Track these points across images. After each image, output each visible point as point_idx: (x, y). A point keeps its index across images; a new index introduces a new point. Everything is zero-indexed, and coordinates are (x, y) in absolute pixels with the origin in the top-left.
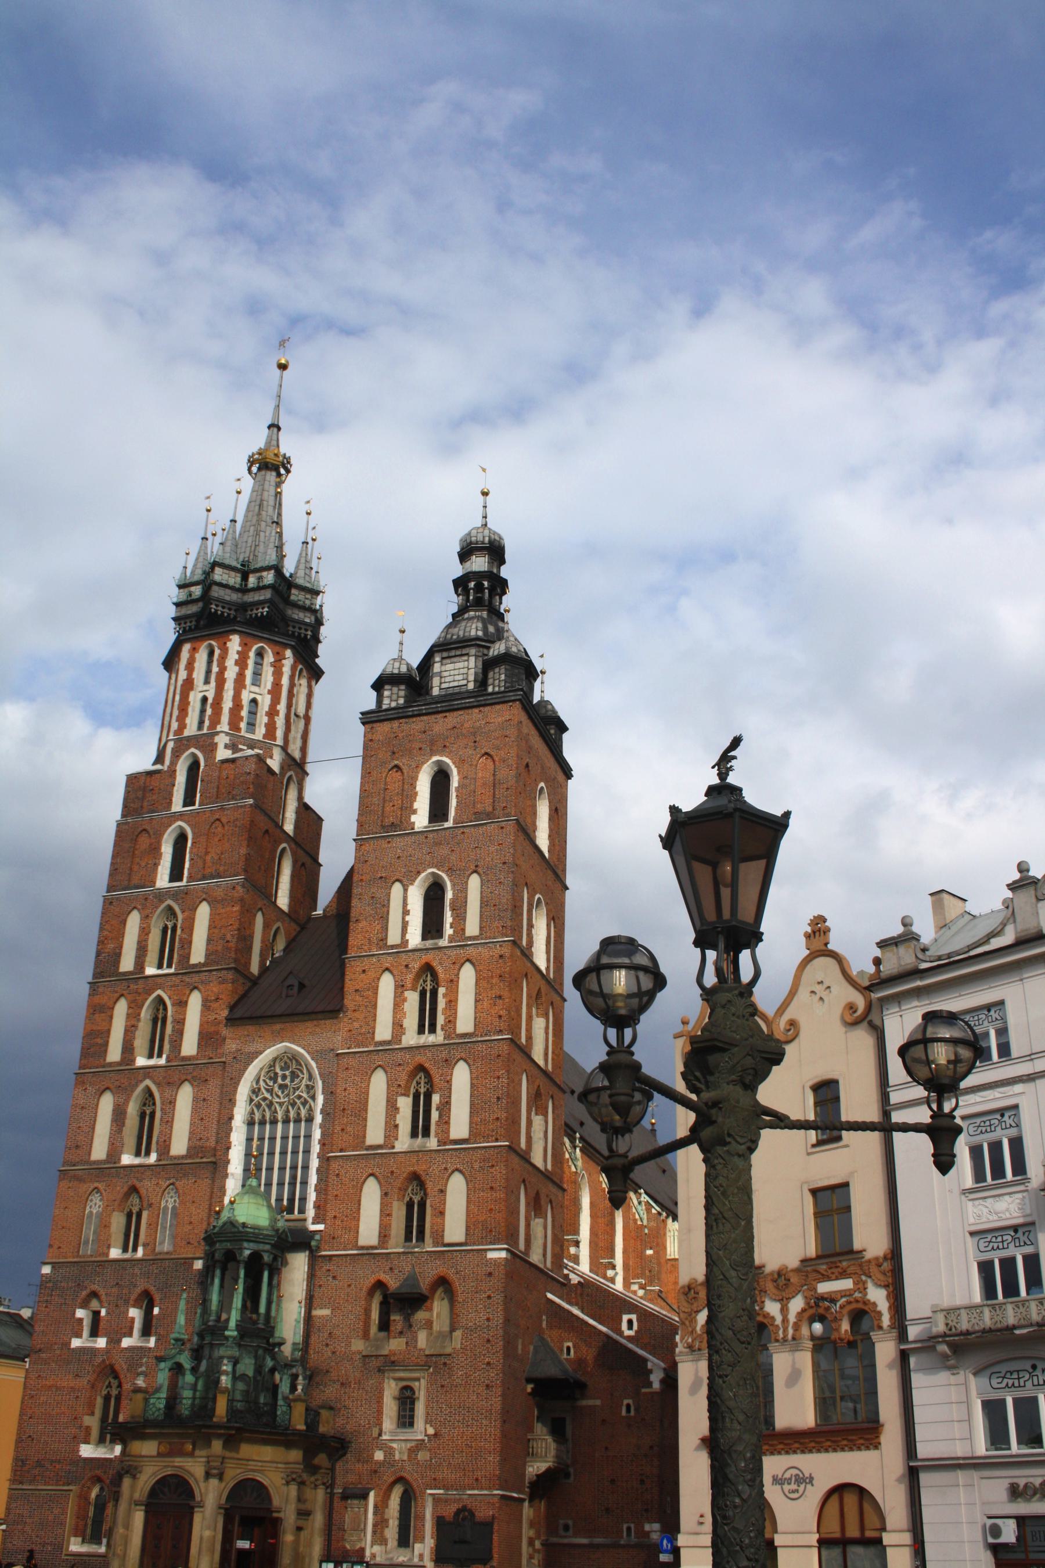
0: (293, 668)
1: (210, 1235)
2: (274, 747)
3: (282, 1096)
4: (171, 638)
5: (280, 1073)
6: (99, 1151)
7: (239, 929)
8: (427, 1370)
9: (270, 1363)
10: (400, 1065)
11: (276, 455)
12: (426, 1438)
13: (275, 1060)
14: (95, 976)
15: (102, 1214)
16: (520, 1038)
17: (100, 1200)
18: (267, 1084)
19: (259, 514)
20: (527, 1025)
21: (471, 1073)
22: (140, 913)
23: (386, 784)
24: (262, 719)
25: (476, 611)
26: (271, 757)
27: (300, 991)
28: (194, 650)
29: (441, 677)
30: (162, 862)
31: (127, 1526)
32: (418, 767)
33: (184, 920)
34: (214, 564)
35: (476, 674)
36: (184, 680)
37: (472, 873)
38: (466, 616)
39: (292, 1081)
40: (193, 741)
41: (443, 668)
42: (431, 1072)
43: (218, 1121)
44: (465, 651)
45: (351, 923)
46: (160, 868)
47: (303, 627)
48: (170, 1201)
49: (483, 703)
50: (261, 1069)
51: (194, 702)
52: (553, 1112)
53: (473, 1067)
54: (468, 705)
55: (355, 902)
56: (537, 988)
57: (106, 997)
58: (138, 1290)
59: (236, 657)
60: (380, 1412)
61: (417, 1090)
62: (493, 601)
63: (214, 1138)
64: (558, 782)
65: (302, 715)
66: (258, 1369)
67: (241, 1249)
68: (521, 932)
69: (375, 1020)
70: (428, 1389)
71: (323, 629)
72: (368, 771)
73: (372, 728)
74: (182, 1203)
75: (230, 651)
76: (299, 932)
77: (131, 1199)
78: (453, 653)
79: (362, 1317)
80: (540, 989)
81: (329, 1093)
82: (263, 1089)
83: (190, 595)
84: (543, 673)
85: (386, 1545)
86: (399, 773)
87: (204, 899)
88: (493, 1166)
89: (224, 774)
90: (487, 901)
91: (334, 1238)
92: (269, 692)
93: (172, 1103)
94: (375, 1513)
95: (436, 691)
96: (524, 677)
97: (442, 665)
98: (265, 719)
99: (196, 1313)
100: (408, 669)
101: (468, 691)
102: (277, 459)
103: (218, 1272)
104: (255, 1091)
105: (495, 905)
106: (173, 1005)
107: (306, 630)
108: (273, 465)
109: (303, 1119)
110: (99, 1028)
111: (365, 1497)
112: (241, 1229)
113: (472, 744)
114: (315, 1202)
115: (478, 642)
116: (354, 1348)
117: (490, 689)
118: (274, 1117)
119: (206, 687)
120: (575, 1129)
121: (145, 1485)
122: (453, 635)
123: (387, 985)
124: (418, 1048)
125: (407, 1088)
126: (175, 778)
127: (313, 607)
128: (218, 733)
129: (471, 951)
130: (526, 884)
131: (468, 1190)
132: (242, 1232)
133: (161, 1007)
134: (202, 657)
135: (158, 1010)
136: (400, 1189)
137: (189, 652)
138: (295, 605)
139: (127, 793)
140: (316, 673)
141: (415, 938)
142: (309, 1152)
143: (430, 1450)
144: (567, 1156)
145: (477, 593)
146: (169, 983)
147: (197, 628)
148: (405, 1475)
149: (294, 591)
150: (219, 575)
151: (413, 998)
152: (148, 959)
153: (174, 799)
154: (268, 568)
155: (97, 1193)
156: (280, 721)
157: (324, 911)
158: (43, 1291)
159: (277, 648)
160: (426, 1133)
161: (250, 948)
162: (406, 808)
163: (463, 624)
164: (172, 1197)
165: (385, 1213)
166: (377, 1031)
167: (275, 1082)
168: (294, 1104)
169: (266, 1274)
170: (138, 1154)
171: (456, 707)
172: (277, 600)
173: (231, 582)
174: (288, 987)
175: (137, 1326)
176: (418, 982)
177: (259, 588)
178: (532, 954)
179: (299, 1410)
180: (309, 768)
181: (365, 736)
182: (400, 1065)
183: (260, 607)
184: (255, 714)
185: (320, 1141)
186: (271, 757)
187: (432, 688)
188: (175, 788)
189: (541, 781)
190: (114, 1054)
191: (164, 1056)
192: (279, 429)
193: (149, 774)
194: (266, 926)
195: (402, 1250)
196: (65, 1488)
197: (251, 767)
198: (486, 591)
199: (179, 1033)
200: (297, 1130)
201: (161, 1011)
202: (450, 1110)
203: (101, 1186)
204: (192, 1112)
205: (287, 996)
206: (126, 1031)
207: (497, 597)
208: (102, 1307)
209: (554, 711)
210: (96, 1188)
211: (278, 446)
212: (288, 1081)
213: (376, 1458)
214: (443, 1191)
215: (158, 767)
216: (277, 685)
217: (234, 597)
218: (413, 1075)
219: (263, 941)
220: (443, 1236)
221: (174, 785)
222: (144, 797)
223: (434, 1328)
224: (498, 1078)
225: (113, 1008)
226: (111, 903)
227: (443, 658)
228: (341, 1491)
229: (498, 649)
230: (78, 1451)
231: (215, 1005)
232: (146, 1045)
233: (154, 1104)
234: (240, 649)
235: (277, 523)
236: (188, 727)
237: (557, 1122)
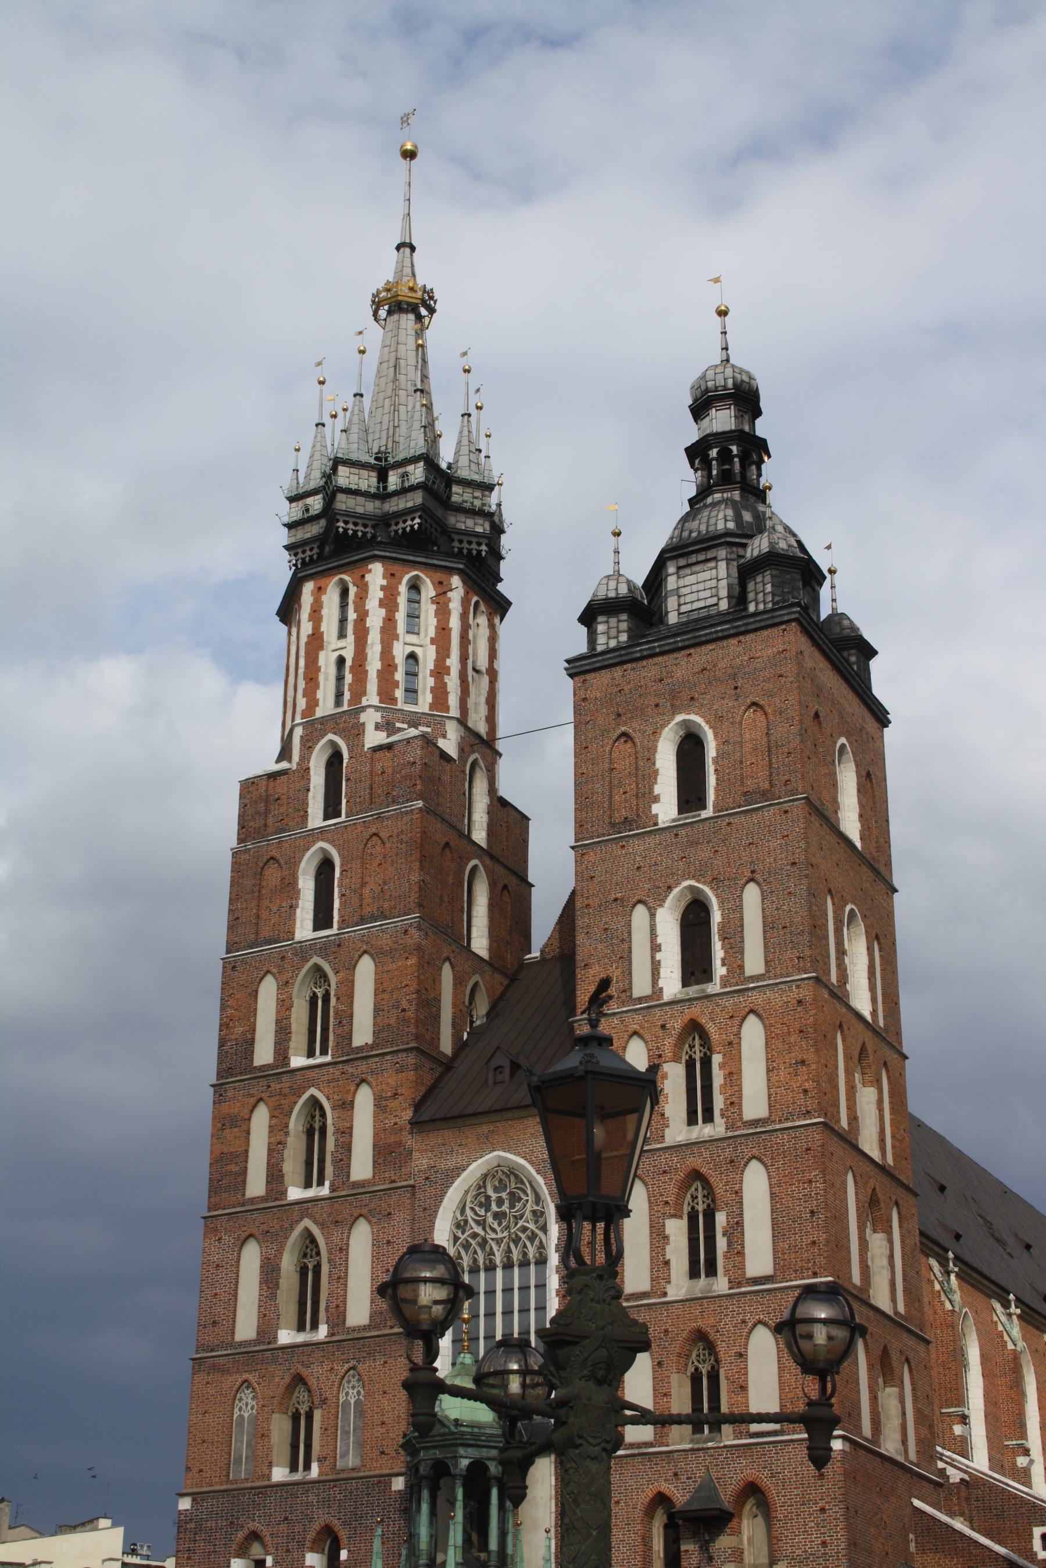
0: (465, 602)
1: (409, 1441)
2: (447, 721)
3: (498, 1229)
4: (285, 575)
5: (494, 1196)
6: (246, 1328)
7: (418, 992)
10: (665, 1172)
11: (411, 289)
13: (485, 1177)
14: (220, 1074)
15: (257, 1418)
16: (839, 1121)
17: (253, 1398)
18: (476, 1214)
19: (395, 380)
20: (847, 1100)
21: (770, 1178)
22: (276, 979)
23: (611, 762)
24: (426, 682)
25: (723, 491)
26: (444, 737)
27: (513, 1073)
28: (320, 590)
29: (679, 597)
30: (300, 902)
32: (656, 733)
33: (339, 984)
34: (337, 462)
35: (730, 587)
36: (309, 636)
37: (748, 882)
38: (709, 500)
39: (512, 1206)
41: (681, 583)
42: (712, 1180)
44: (710, 554)
45: (578, 970)
46: (298, 911)
47: (474, 540)
48: (351, 1394)
49: (743, 629)
50: (467, 1192)
51: (326, 666)
52: (900, 1227)
53: (772, 1169)
54: (720, 634)
55: (581, 939)
56: (860, 1044)
57: (238, 1105)
58: (317, 1526)
59: (381, 594)
61: (693, 1208)
62: (748, 474)
64: (867, 733)
65: (483, 669)
67: (456, 1458)
68: (827, 964)
71: (505, 540)
72: (584, 745)
73: (585, 680)
74: (368, 1395)
75: (371, 588)
76: (508, 987)
77: (296, 1394)
78: (693, 559)
79: (640, 1549)
80: (864, 1043)
82: (470, 1220)
83: (307, 510)
84: (832, 572)
86: (629, 744)
87: (365, 952)
89: (378, 767)
90: (773, 923)
92: (433, 641)
95: (673, 618)
96: (800, 584)
97: (679, 578)
98: (431, 682)
99: (400, 1555)
100: (629, 590)
101: (720, 614)
102: (414, 295)
103: (425, 1494)
105: (784, 927)
106: (333, 1108)
107: (479, 544)
108: (408, 303)
109: (532, 1260)
110: (232, 1150)
112: (453, 1429)
113: (733, 692)
117: (752, 608)
118: (491, 1260)
119: (341, 643)
120: (947, 1245)
122: (691, 532)
124: (688, 1145)
125: (679, 1205)
126: (309, 779)
127: (486, 508)
128: (363, 709)
129: (755, 998)
130: (830, 891)
132: (454, 1433)
133: (317, 1113)
135: (313, 1117)
136: (679, 1355)
137: (312, 594)
138: (460, 509)
139: (243, 806)
140: (500, 606)
141: (671, 984)
142: (545, 1308)
144: (937, 1287)
145: (723, 464)
146: (326, 1078)
147: (321, 557)
150: (345, 477)
152: (292, 1044)
153: (310, 810)
154: (414, 460)
155: (247, 1388)
156: (452, 682)
157: (542, 951)
158: (182, 1535)
159: (439, 576)
160: (711, 1270)
161: (436, 1018)
162: (644, 795)
163: (706, 513)
164: (353, 1387)
167: (487, 1210)
168: (516, 1240)
169: (494, 1493)
170: (301, 1328)
171: (703, 639)
172: (432, 505)
173: (364, 486)
174: (496, 1069)
176: (682, 1049)
177: (403, 491)
178: (847, 994)
180: (500, 746)
181: (575, 695)
182: (665, 1172)
183: (409, 518)
186: (444, 737)
187: (667, 613)
188: (311, 794)
189: (841, 735)
190: (256, 1185)
191: (327, 1183)
192: (413, 249)
193: (273, 776)
194: (458, 982)
195: (690, 1446)
197: (416, 753)
198: (736, 460)
200: (524, 1277)
201: (317, 1118)
203: (252, 1378)
204: (373, 1262)
205: (495, 1083)
206: (270, 1152)
207: (754, 467)
208: (267, 1553)
209: (853, 628)
210: (246, 1381)
211: (414, 275)
212: (505, 1208)
214: (742, 1355)
215: (284, 765)
216: (443, 630)
217: (370, 507)
218: (684, 1186)
219: (455, 1005)
221: (308, 790)
222: (267, 811)
223: (746, 1561)
224: (810, 1181)
225: (249, 1119)
226: (234, 967)
227: (679, 568)
229: (759, 545)
231: (393, 1104)
232: (301, 1168)
233: (318, 1254)
234: (384, 582)
235: (422, 391)
236: (321, 703)
237: (908, 1241)
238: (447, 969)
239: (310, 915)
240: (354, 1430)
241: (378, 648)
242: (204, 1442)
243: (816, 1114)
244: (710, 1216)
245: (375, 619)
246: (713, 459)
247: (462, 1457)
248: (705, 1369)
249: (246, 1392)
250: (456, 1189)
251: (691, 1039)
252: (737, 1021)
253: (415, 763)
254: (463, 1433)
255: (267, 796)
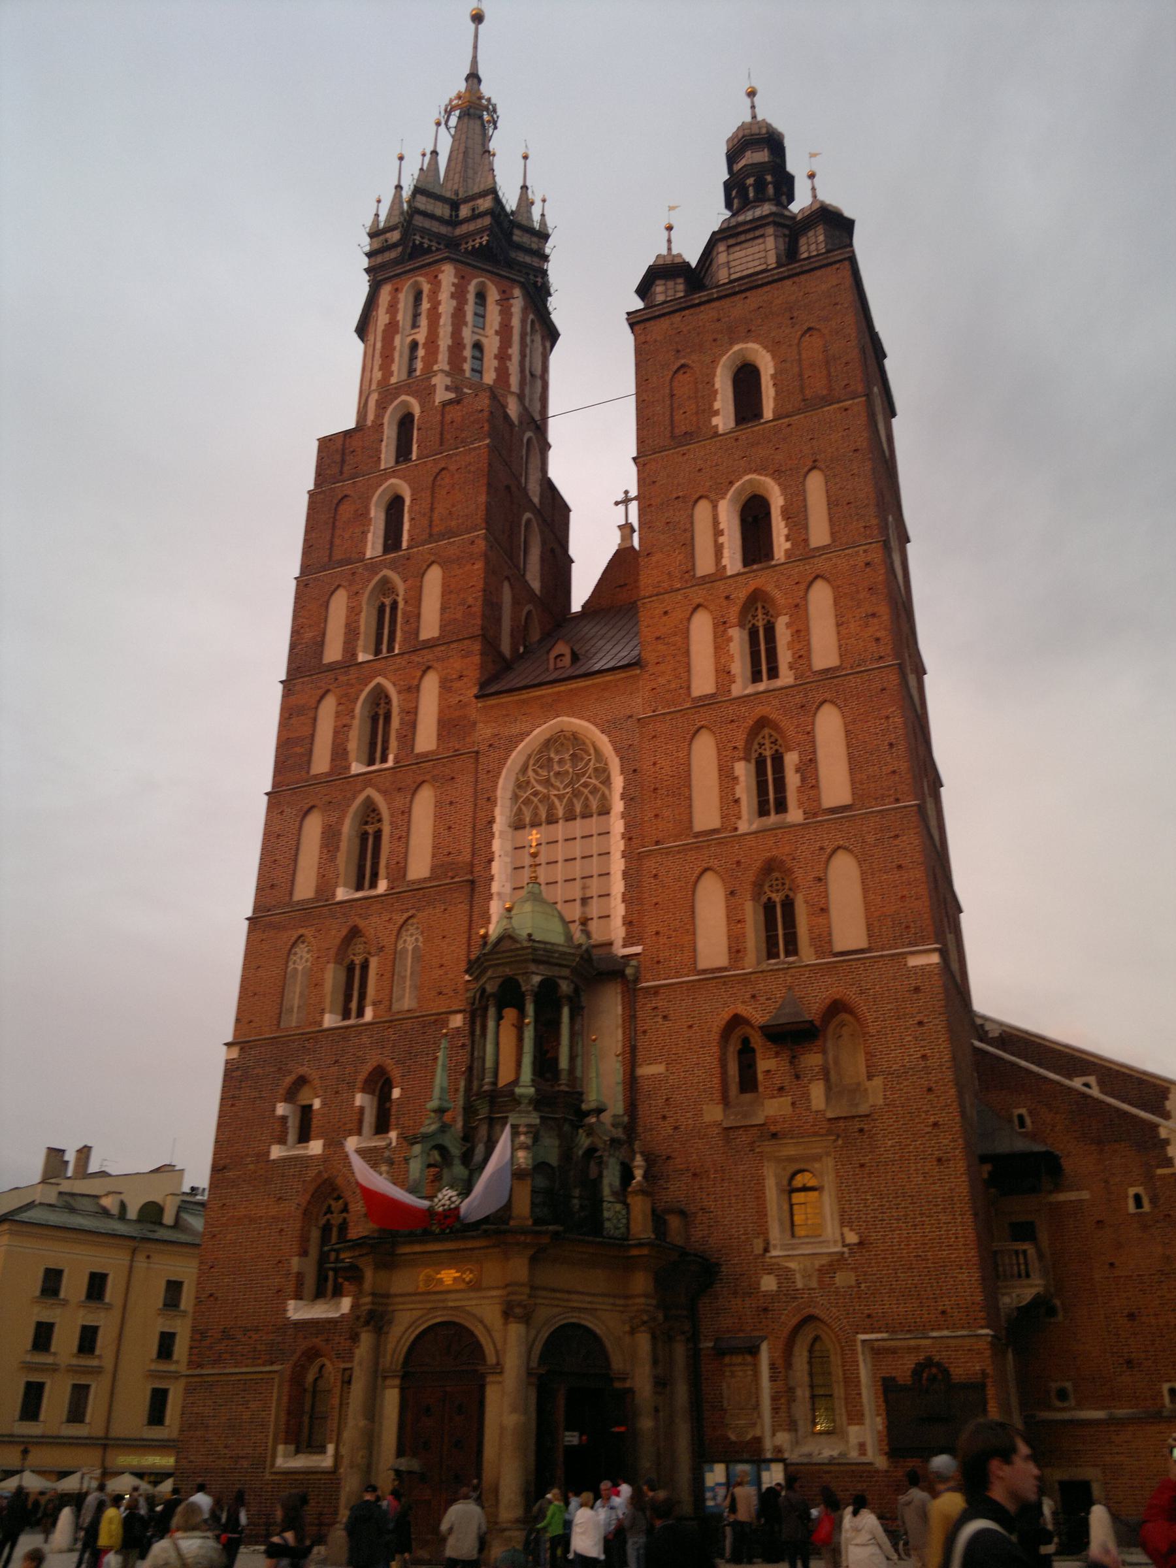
0: (525, 310)
6: (305, 888)
7: (485, 591)
8: (835, 1141)
9: (584, 1141)
10: (732, 721)
12: (846, 1250)
17: (308, 952)
21: (844, 717)
23: (671, 390)
29: (729, 268)
31: (372, 1412)
32: (715, 362)
36: (386, 325)
37: (810, 470)
39: (574, 766)
40: (399, 389)
41: (731, 257)
42: (782, 724)
43: (474, 829)
44: (757, 233)
45: (640, 559)
46: (370, 536)
50: (530, 756)
54: (776, 277)
59: (453, 289)
60: (762, 1214)
61: (760, 754)
63: (469, 850)
66: (566, 1154)
69: (689, 671)
70: (837, 1172)
72: (646, 378)
78: (742, 238)
79: (717, 1071)
81: (631, 773)
82: (533, 781)
83: (386, 241)
85: (796, 1431)
86: (688, 375)
87: (433, 562)
88: (897, 836)
91: (658, 962)
92: (497, 333)
93: (407, 812)
94: (773, 1379)
97: (729, 254)
98: (495, 363)
104: (521, 785)
106: (399, 692)
107: (536, 277)
111: (754, 1351)
113: (790, 321)
114: (624, 917)
115: (777, 219)
116: (707, 1118)
121: (398, 1342)
123: (701, 628)
128: (435, 373)
129: (820, 564)
131: (863, 873)
134: (405, 299)
135: (378, 705)
137: (390, 293)
138: (520, 247)
140: (551, 335)
141: (732, 561)
143: (854, 1269)
148: (817, 1312)
149: (516, 232)
150: (422, 203)
151: (738, 638)
152: (361, 643)
154: (483, 194)
155: (303, 942)
160: (781, 807)
162: (704, 411)
164: (412, 935)
165: (734, 919)
166: (694, 686)
169: (566, 1012)
170: (359, 887)
171: (760, 282)
174: (556, 657)
175: (369, 1119)
177: (475, 216)
179: (639, 1206)
182: (732, 721)
183: (478, 237)
184: (481, 359)
185: (623, 836)
188: (384, 444)
190: (321, 763)
191: (391, 757)
194: (516, 602)
196: (268, 1368)
199: (411, 726)
201: (382, 705)
202: (816, 769)
206: (336, 733)
210: (301, 936)
213: (763, 1289)
217: (443, 230)
219: (513, 619)
220: (830, 942)
222: (343, 461)
224: (887, 718)
225: (316, 708)
227: (729, 247)
228: (711, 1344)
230: (285, 1311)
231: (457, 685)
232: (366, 748)
233: (380, 820)
234: (456, 281)
238: (506, 584)
239: (380, 541)
240: (412, 973)
241: (449, 329)
242: (255, 994)
243: (890, 659)
244: (778, 760)
245: (446, 306)
246: (750, 185)
247: (533, 973)
248: (777, 898)
249: (302, 946)
250: (519, 752)
251: (753, 609)
252: (803, 586)
253: (482, 410)
254: (535, 949)
255: (343, 450)
